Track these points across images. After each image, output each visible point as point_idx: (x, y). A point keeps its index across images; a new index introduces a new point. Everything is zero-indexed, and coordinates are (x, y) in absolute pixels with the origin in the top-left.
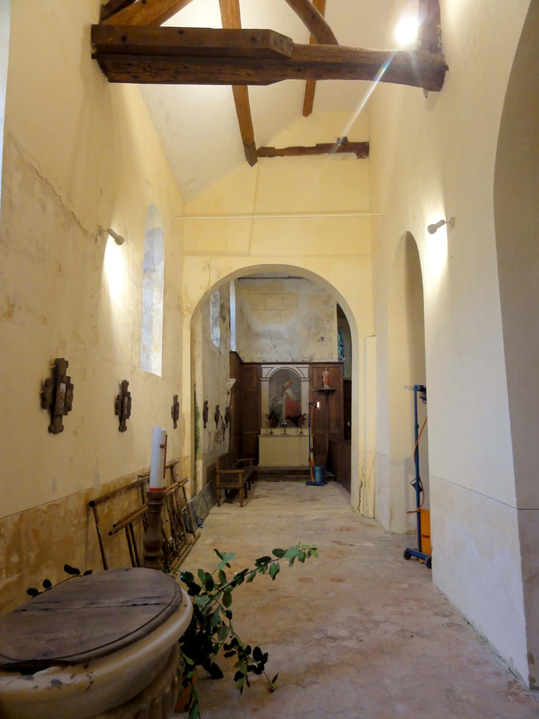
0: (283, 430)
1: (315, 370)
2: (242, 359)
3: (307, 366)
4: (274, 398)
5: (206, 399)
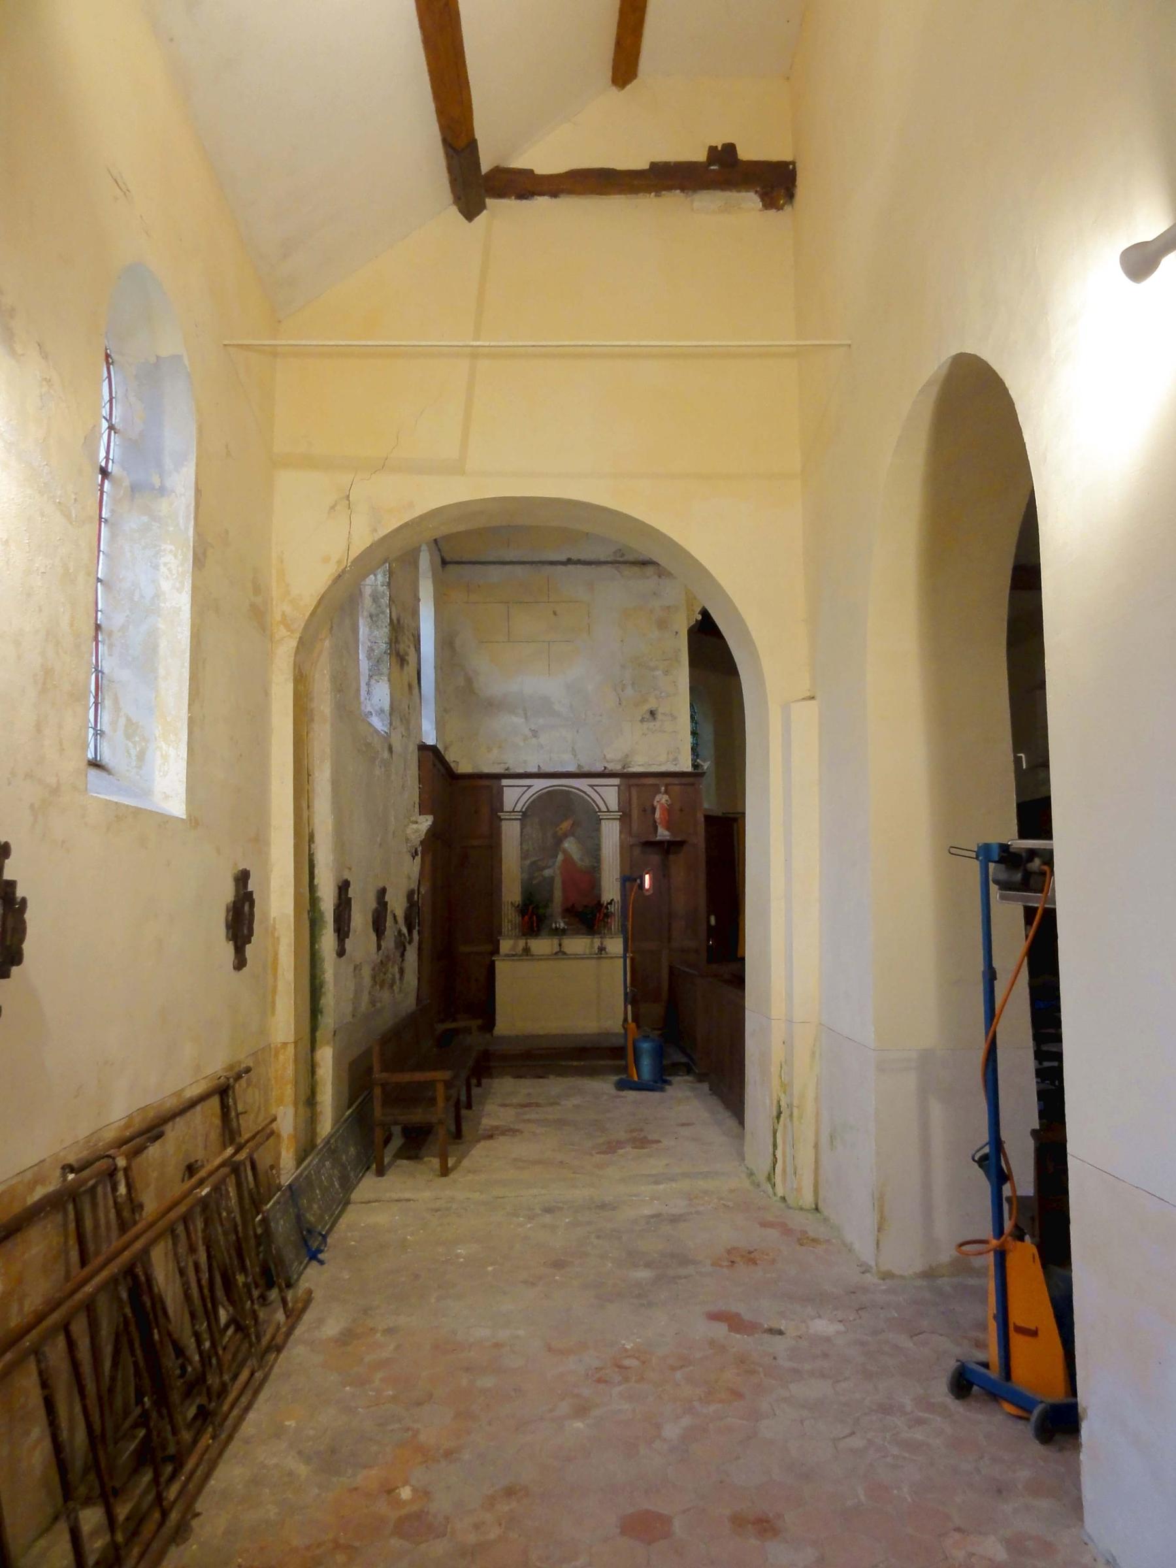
0: (556, 941)
1: (634, 792)
2: (453, 765)
3: (616, 781)
4: (533, 863)
5: (347, 875)
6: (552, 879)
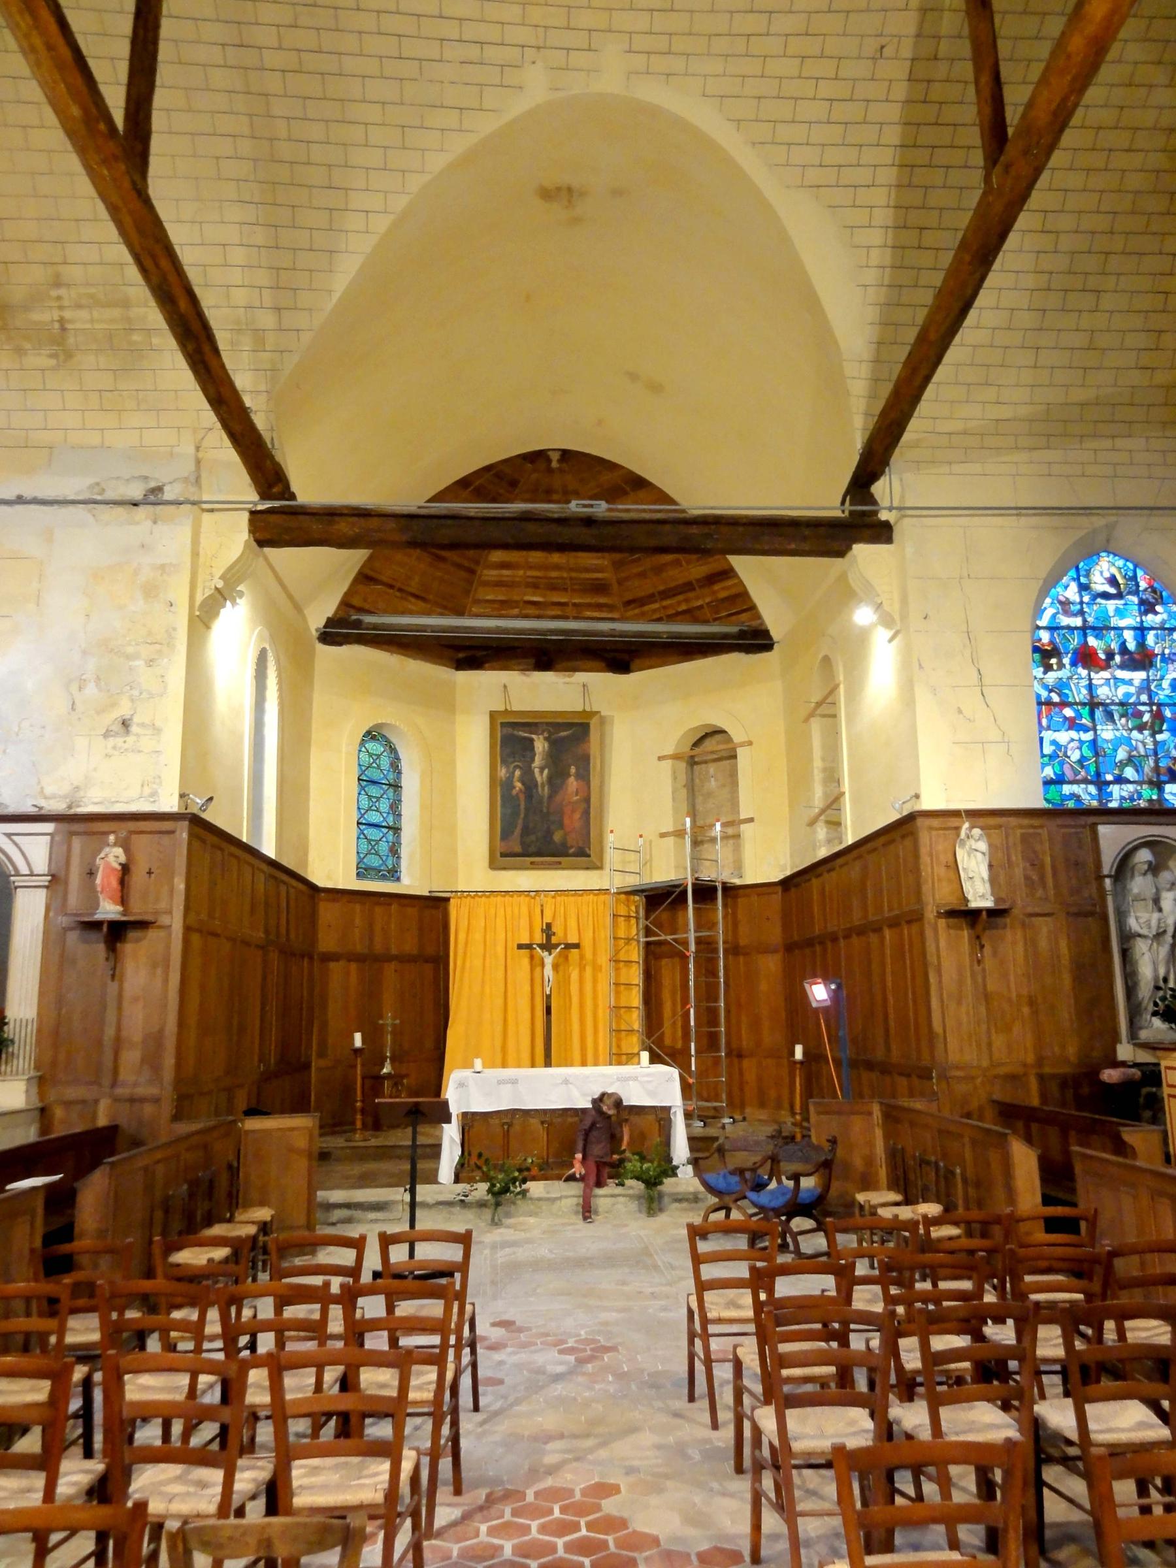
3: (49, 827)
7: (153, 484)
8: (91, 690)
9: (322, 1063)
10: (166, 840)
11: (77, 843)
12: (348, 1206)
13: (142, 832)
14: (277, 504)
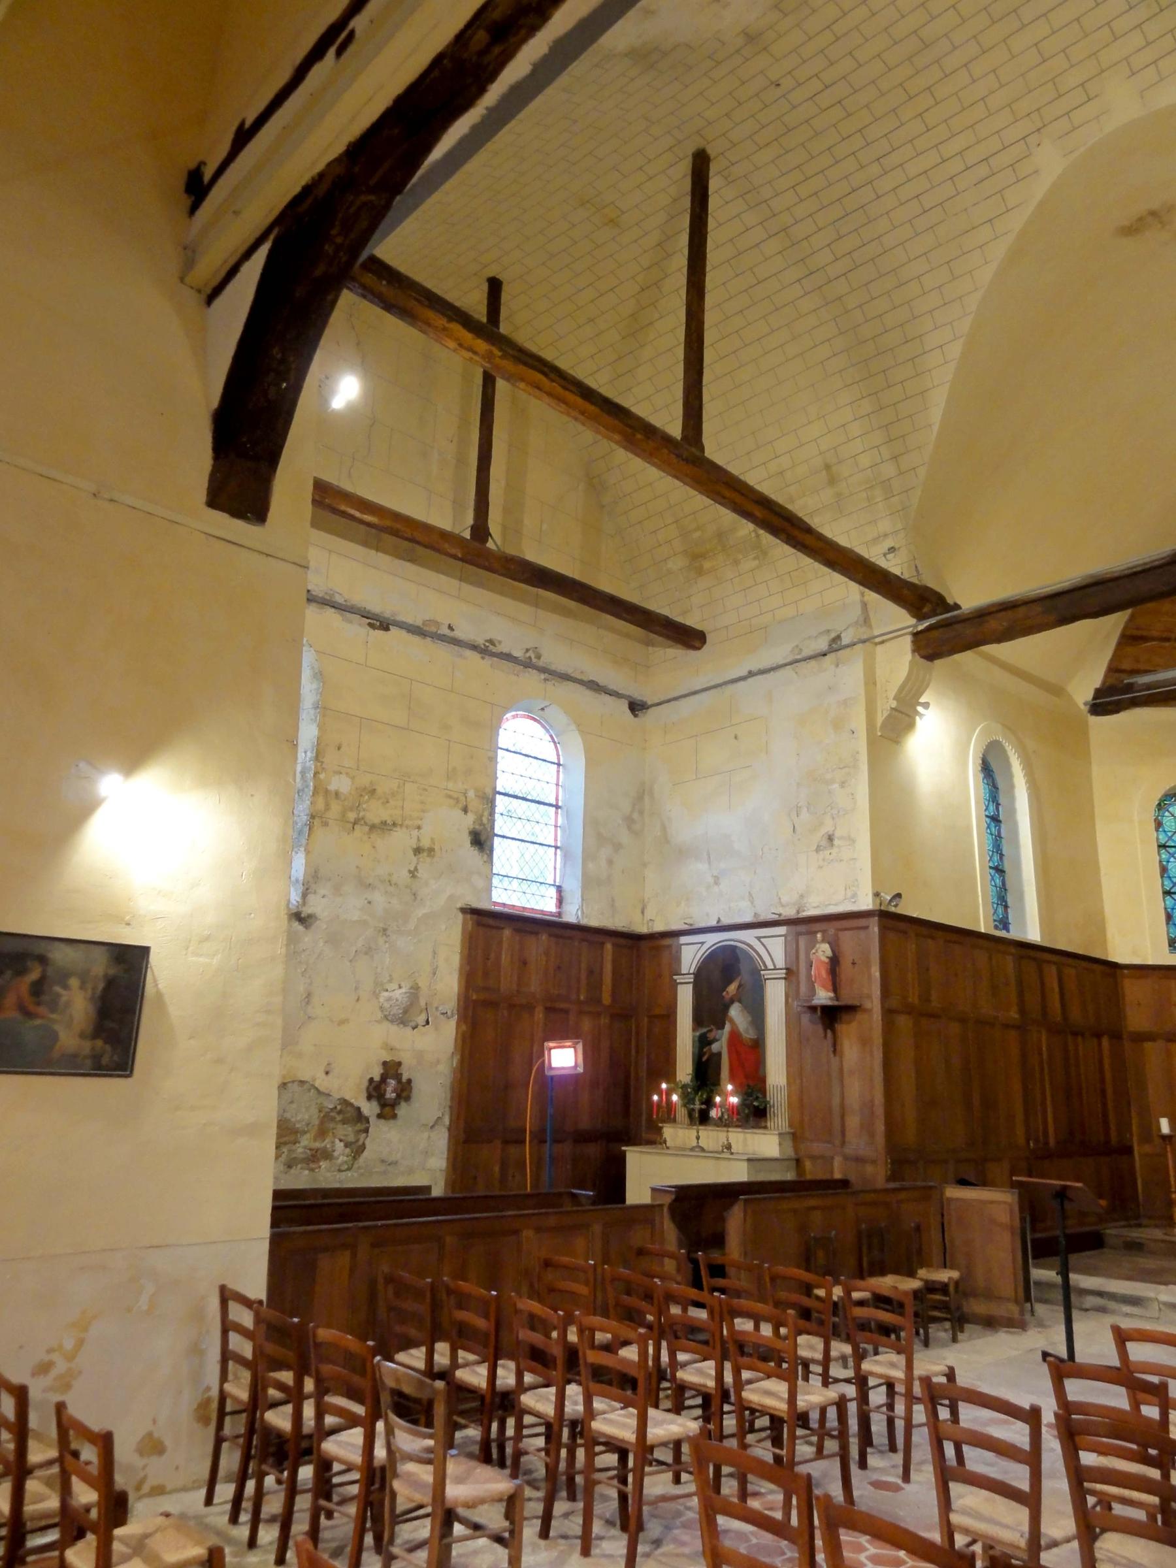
3: (782, 930)
6: (719, 1054)
7: (833, 635)
8: (805, 815)
9: (1147, 1148)
10: (862, 934)
11: (802, 941)
12: (1100, 1294)
13: (846, 929)
14: (933, 621)
